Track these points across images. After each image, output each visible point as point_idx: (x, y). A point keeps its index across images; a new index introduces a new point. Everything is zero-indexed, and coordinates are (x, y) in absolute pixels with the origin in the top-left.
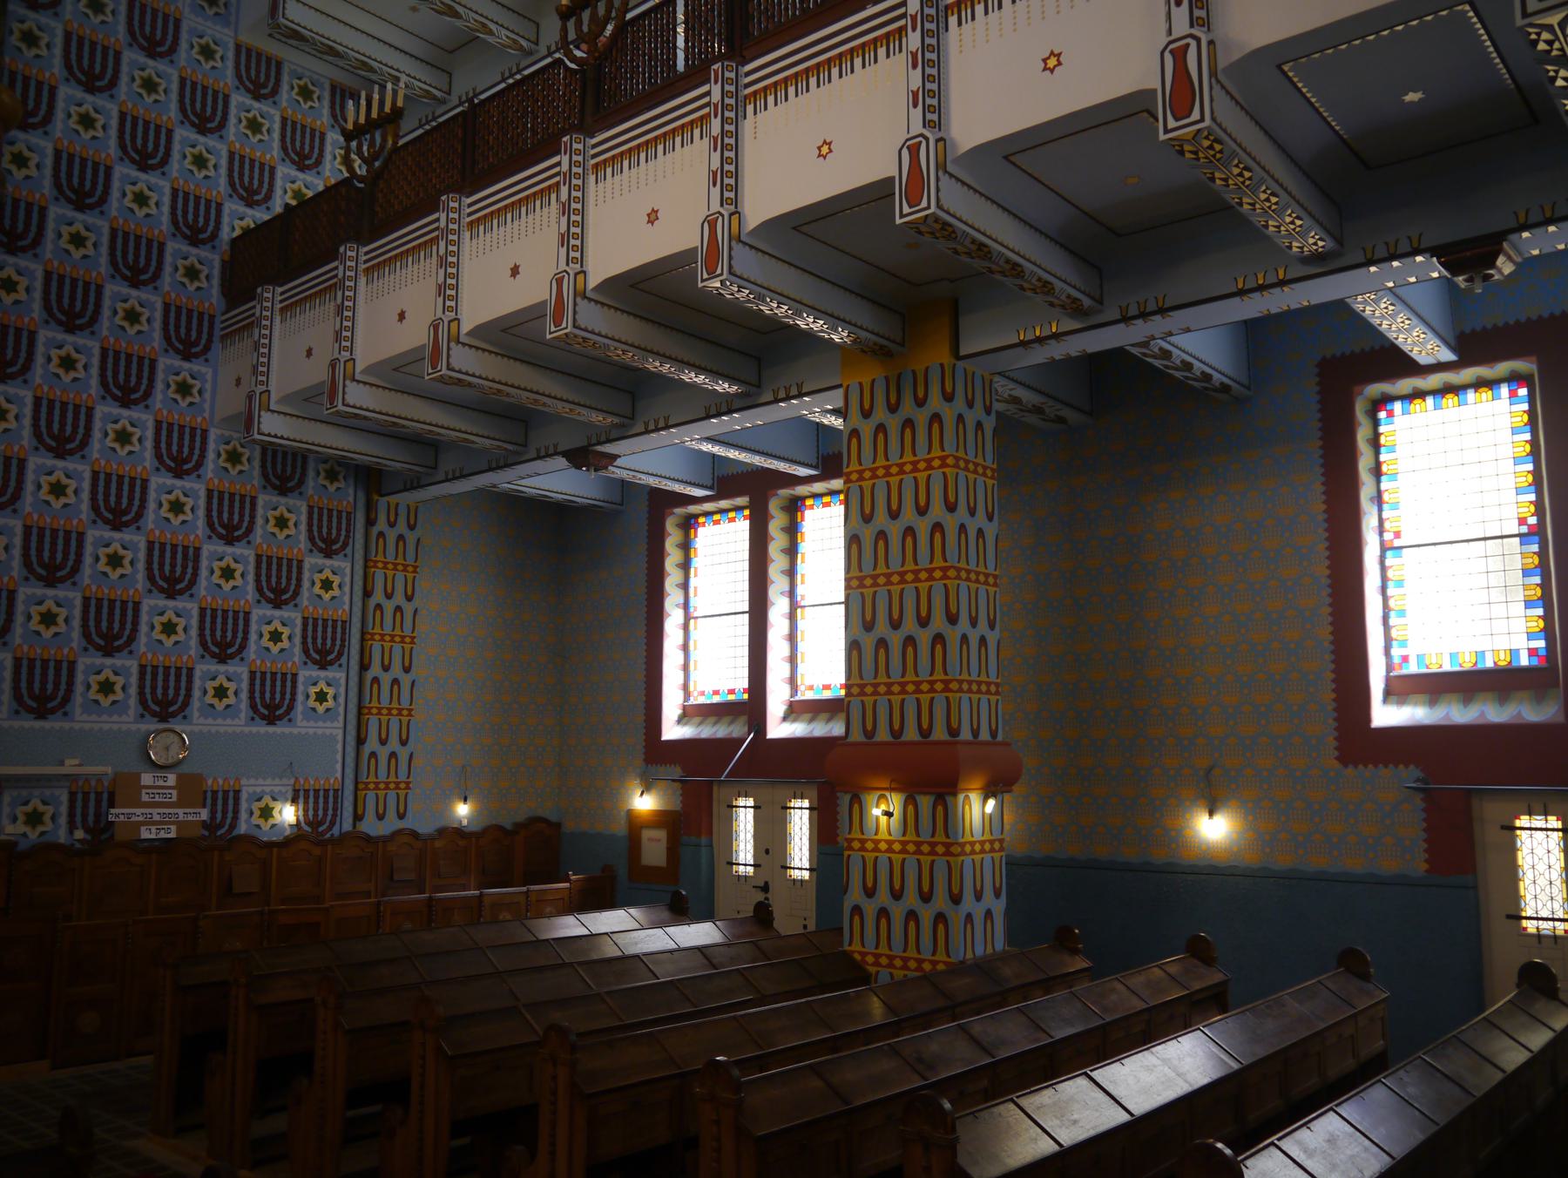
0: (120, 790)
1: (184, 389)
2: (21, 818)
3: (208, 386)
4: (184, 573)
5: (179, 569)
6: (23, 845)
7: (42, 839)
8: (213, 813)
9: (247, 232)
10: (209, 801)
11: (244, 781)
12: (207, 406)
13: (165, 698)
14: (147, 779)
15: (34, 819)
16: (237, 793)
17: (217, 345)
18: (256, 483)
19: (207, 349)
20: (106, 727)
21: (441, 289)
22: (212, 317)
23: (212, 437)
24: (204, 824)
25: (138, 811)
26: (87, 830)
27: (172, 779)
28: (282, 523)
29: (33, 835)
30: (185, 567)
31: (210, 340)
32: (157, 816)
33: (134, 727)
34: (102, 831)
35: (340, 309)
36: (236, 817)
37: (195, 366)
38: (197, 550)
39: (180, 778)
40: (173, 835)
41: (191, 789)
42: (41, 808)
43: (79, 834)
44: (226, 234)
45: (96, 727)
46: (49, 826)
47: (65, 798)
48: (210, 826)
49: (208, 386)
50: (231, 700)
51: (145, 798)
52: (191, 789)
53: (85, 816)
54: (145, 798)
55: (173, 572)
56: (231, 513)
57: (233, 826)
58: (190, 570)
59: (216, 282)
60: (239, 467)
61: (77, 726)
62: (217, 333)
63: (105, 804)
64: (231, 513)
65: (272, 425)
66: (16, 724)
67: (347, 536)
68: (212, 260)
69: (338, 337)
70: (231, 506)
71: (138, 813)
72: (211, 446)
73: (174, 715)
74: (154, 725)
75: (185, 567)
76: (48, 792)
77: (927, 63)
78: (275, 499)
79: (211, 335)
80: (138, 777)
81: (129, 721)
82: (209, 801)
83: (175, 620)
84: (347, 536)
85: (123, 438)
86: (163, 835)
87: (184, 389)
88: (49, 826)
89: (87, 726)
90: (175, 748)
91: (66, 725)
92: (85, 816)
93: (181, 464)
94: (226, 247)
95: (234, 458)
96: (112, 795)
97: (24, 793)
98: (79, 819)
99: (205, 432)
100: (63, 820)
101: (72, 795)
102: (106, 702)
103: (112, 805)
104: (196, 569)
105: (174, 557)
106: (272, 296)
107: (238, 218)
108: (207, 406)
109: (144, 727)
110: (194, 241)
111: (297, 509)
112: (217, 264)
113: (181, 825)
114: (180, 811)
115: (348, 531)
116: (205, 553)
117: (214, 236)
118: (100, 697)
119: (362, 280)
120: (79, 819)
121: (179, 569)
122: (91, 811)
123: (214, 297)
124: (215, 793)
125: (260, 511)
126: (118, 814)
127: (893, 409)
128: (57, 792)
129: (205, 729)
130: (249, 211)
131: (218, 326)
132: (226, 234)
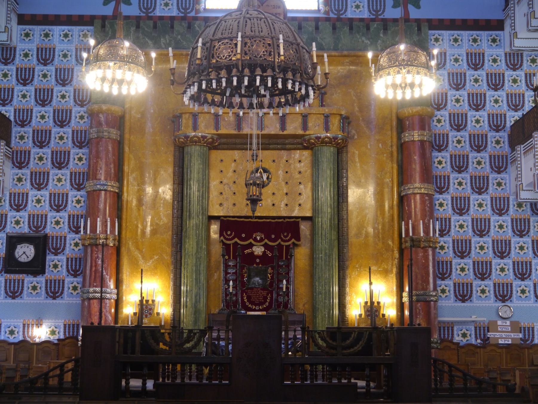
0: (490, 327)
1: (499, 184)
2: (460, 335)
3: (508, 181)
4: (506, 249)
5: (504, 249)
6: (461, 344)
7: (468, 342)
8: (525, 335)
9: (516, 122)
10: (522, 331)
11: (535, 324)
12: (508, 189)
13: (503, 294)
14: (499, 323)
15: (464, 335)
16: (533, 328)
18: (529, 213)
19: (506, 168)
20: (484, 305)
22: (507, 156)
24: (521, 339)
25: (498, 334)
26: (481, 340)
27: (508, 323)
29: (465, 341)
30: (506, 248)
31: (507, 165)
32: (504, 336)
33: (494, 305)
34: (486, 340)
36: (533, 337)
37: (502, 175)
38: (510, 241)
39: (511, 322)
40: (510, 342)
41: (516, 327)
42: (466, 332)
43: (479, 341)
44: (508, 125)
45: (481, 305)
46: (469, 338)
47: (473, 329)
48: (524, 340)
49: (508, 181)
50: (528, 294)
51: (499, 329)
52: (516, 327)
53: (480, 335)
54: (499, 329)
55: (502, 250)
56: (521, 226)
57: (532, 340)
58: (508, 249)
59: (507, 143)
60: (522, 209)
61: (475, 305)
62: (509, 161)
63: (486, 331)
64: (521, 226)
65: (524, 195)
66: (456, 304)
68: (504, 135)
70: (521, 223)
71: (497, 335)
73: (507, 300)
74: (500, 304)
75: (506, 248)
76: (468, 327)
80: (496, 322)
81: (491, 302)
82: (522, 331)
83: (504, 266)
85: (481, 206)
86: (506, 342)
88: (469, 338)
89: (478, 305)
90: (508, 312)
91: (472, 305)
92: (480, 335)
93: (501, 211)
96: (488, 328)
97: (461, 327)
98: (478, 336)
99: (508, 198)
100: (473, 336)
101: (476, 328)
102: (483, 296)
103: (488, 331)
104: (510, 248)
105: (502, 244)
106: (520, 149)
107: (512, 117)
108: (508, 189)
109: (497, 305)
110: (497, 131)
112: (506, 136)
113: (513, 339)
114: (512, 334)
116: (512, 242)
117: (504, 126)
118: (481, 295)
120: (478, 336)
121: (504, 249)
122: (482, 333)
124: (524, 328)
125: (531, 224)
126: (490, 335)
128: (471, 327)
129: (519, 305)
130: (516, 113)
131: (509, 159)
132: (508, 125)
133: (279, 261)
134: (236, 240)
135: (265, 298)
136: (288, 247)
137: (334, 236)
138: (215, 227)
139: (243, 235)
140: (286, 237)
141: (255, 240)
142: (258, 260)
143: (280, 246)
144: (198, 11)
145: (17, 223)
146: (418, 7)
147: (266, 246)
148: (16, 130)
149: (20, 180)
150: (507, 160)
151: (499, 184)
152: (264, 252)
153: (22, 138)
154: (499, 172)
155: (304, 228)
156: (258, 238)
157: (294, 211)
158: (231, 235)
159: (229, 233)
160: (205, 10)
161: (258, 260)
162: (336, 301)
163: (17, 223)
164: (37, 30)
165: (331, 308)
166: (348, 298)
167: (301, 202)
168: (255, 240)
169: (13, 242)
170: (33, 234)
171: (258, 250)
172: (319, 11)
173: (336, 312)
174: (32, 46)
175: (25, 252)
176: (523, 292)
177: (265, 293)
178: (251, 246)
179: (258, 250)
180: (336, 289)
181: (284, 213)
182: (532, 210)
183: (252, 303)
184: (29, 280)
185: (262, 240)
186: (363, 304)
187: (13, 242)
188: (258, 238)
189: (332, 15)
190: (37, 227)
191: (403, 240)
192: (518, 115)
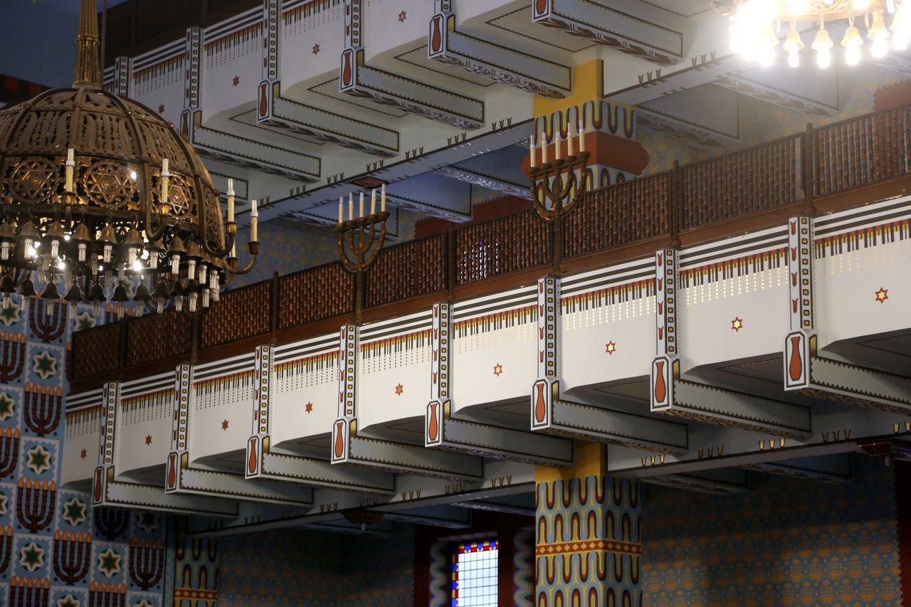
3: (56, 455)
12: (55, 472)
17: (63, 421)
19: (56, 425)
21: (257, 415)
22: (59, 398)
23: (59, 496)
31: (58, 418)
35: (177, 415)
37: (47, 440)
49: (56, 455)
59: (62, 369)
62: (64, 411)
67: (160, 571)
68: (59, 351)
69: (175, 435)
72: (58, 504)
77: (548, 336)
78: (104, 544)
79: (58, 413)
84: (160, 571)
87: (39, 459)
94: (69, 339)
95: (74, 512)
99: (54, 493)
108: (55, 472)
111: (122, 553)
112: (63, 354)
115: (161, 566)
117: (61, 331)
123: (62, 383)
127: (567, 504)
131: (64, 405)
150: (59, 407)
151: (39, 459)
154: (41, 433)
182: (97, 524)
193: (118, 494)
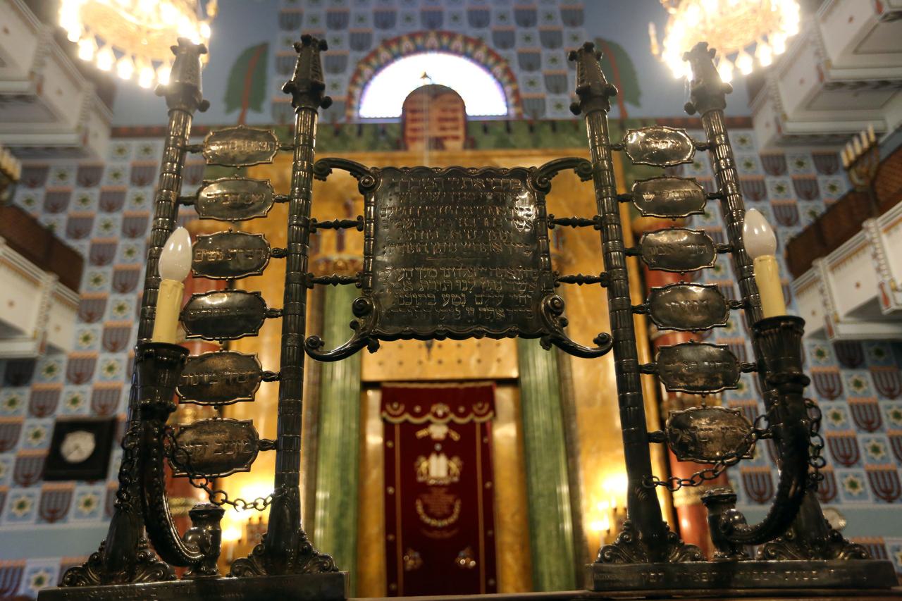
28: (858, 384)
106: (822, 264)
119: (884, 237)
133: (471, 447)
134: (407, 417)
135: (451, 507)
136: (483, 425)
137: (556, 404)
138: (374, 396)
139: (418, 409)
140: (481, 409)
141: (435, 415)
142: (438, 447)
143: (472, 423)
144: (349, 118)
145: (75, 401)
146: (636, 103)
147: (451, 425)
148: (89, 271)
149: (86, 339)
152: (448, 435)
153: (97, 280)
155: (504, 396)
156: (440, 412)
157: (488, 369)
158: (398, 408)
159: (395, 405)
160: (360, 118)
161: (438, 447)
162: (566, 508)
163: (75, 401)
164: (134, 145)
165: (559, 519)
166: (584, 503)
167: (500, 355)
168: (435, 415)
169: (64, 429)
170: (96, 417)
171: (438, 431)
172: (508, 115)
173: (568, 526)
174: (125, 165)
175: (80, 447)
176: (853, 485)
177: (450, 498)
178: (427, 424)
179: (438, 431)
180: (564, 489)
181: (475, 373)
183: (432, 516)
184: (80, 491)
185: (445, 415)
186: (611, 512)
187: (64, 429)
188: (440, 412)
189: (526, 117)
190: (104, 407)
191: (665, 405)
192: (820, 207)
193: (849, 330)
